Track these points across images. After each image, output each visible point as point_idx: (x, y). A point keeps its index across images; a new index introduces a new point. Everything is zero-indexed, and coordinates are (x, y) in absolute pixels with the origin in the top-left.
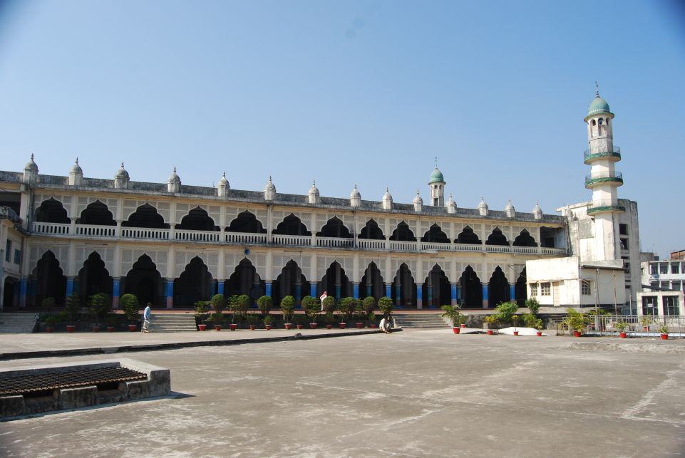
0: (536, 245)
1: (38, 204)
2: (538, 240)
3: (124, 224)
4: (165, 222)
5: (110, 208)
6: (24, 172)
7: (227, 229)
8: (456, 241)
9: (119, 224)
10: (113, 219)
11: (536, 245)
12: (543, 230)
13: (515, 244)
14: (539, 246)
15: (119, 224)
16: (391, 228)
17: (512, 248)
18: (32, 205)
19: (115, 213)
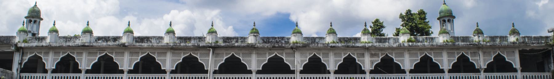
0: (515, 70)
1: (26, 59)
2: (517, 64)
3: (87, 72)
4: (120, 68)
5: (78, 59)
6: (15, 35)
7: (172, 72)
8: (411, 71)
9: (83, 72)
10: (80, 68)
11: (515, 70)
12: (522, 54)
13: (486, 71)
14: (519, 71)
15: (83, 72)
16: (336, 62)
17: (482, 75)
18: (22, 60)
19: (81, 63)
